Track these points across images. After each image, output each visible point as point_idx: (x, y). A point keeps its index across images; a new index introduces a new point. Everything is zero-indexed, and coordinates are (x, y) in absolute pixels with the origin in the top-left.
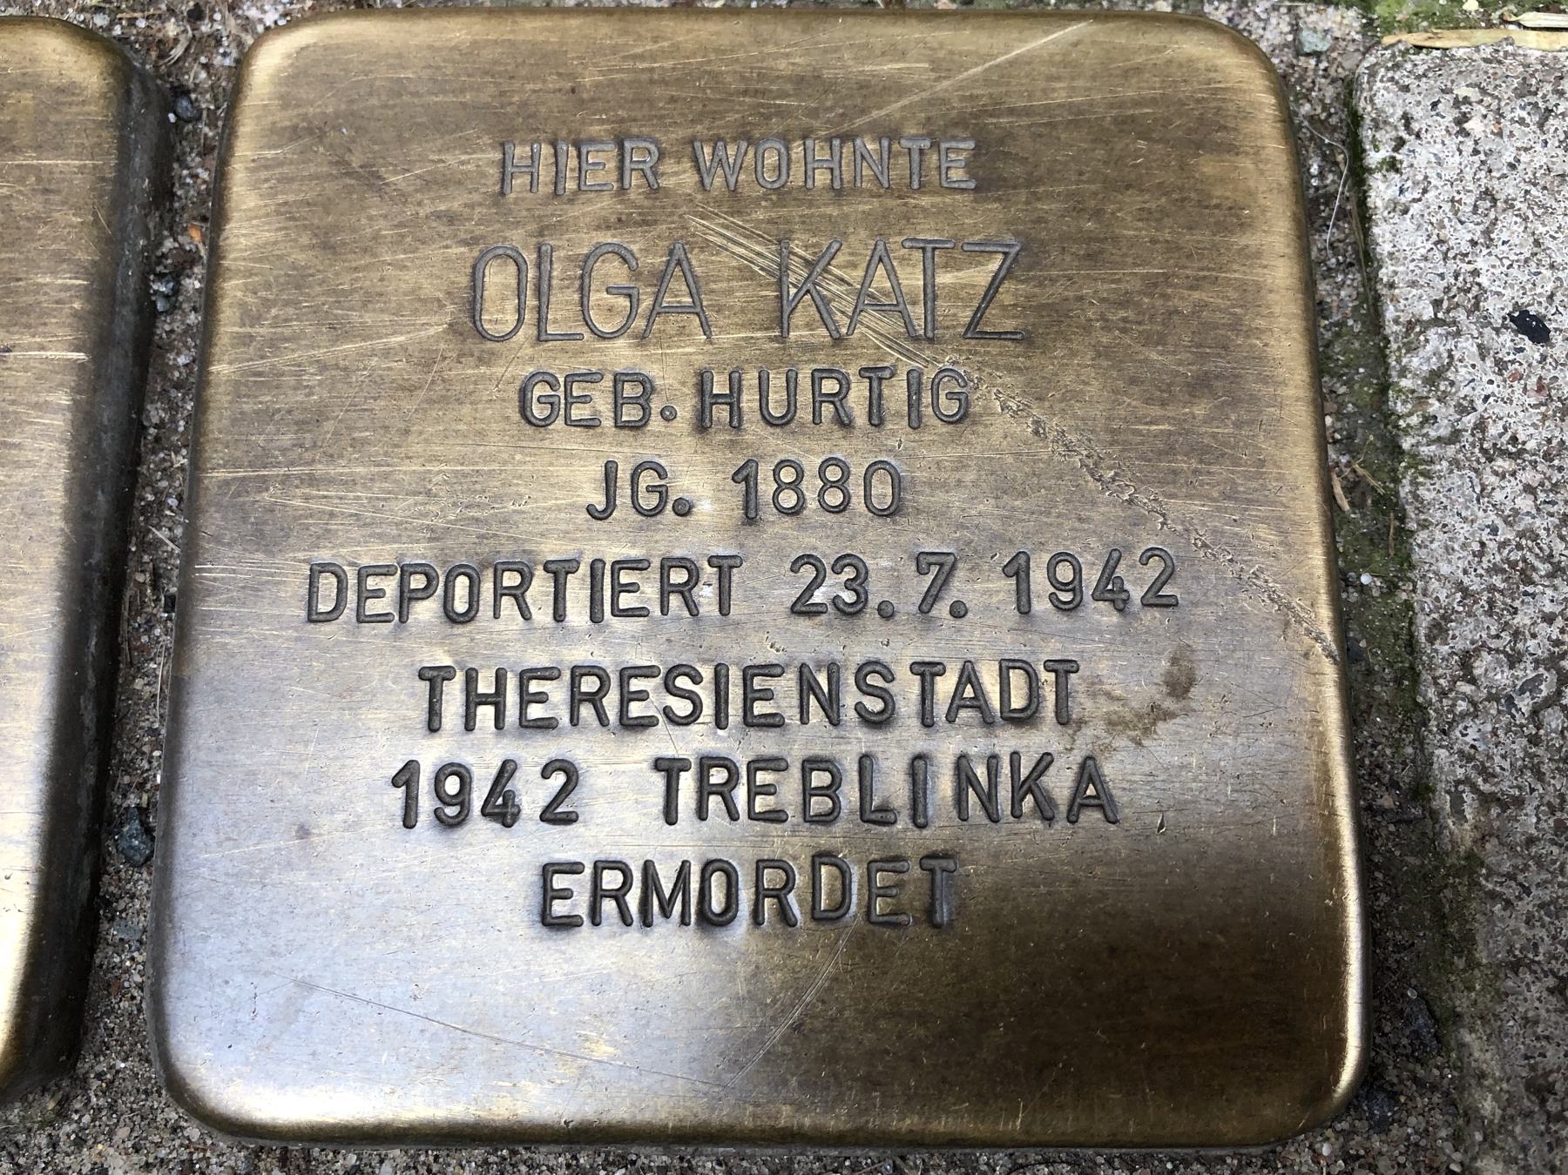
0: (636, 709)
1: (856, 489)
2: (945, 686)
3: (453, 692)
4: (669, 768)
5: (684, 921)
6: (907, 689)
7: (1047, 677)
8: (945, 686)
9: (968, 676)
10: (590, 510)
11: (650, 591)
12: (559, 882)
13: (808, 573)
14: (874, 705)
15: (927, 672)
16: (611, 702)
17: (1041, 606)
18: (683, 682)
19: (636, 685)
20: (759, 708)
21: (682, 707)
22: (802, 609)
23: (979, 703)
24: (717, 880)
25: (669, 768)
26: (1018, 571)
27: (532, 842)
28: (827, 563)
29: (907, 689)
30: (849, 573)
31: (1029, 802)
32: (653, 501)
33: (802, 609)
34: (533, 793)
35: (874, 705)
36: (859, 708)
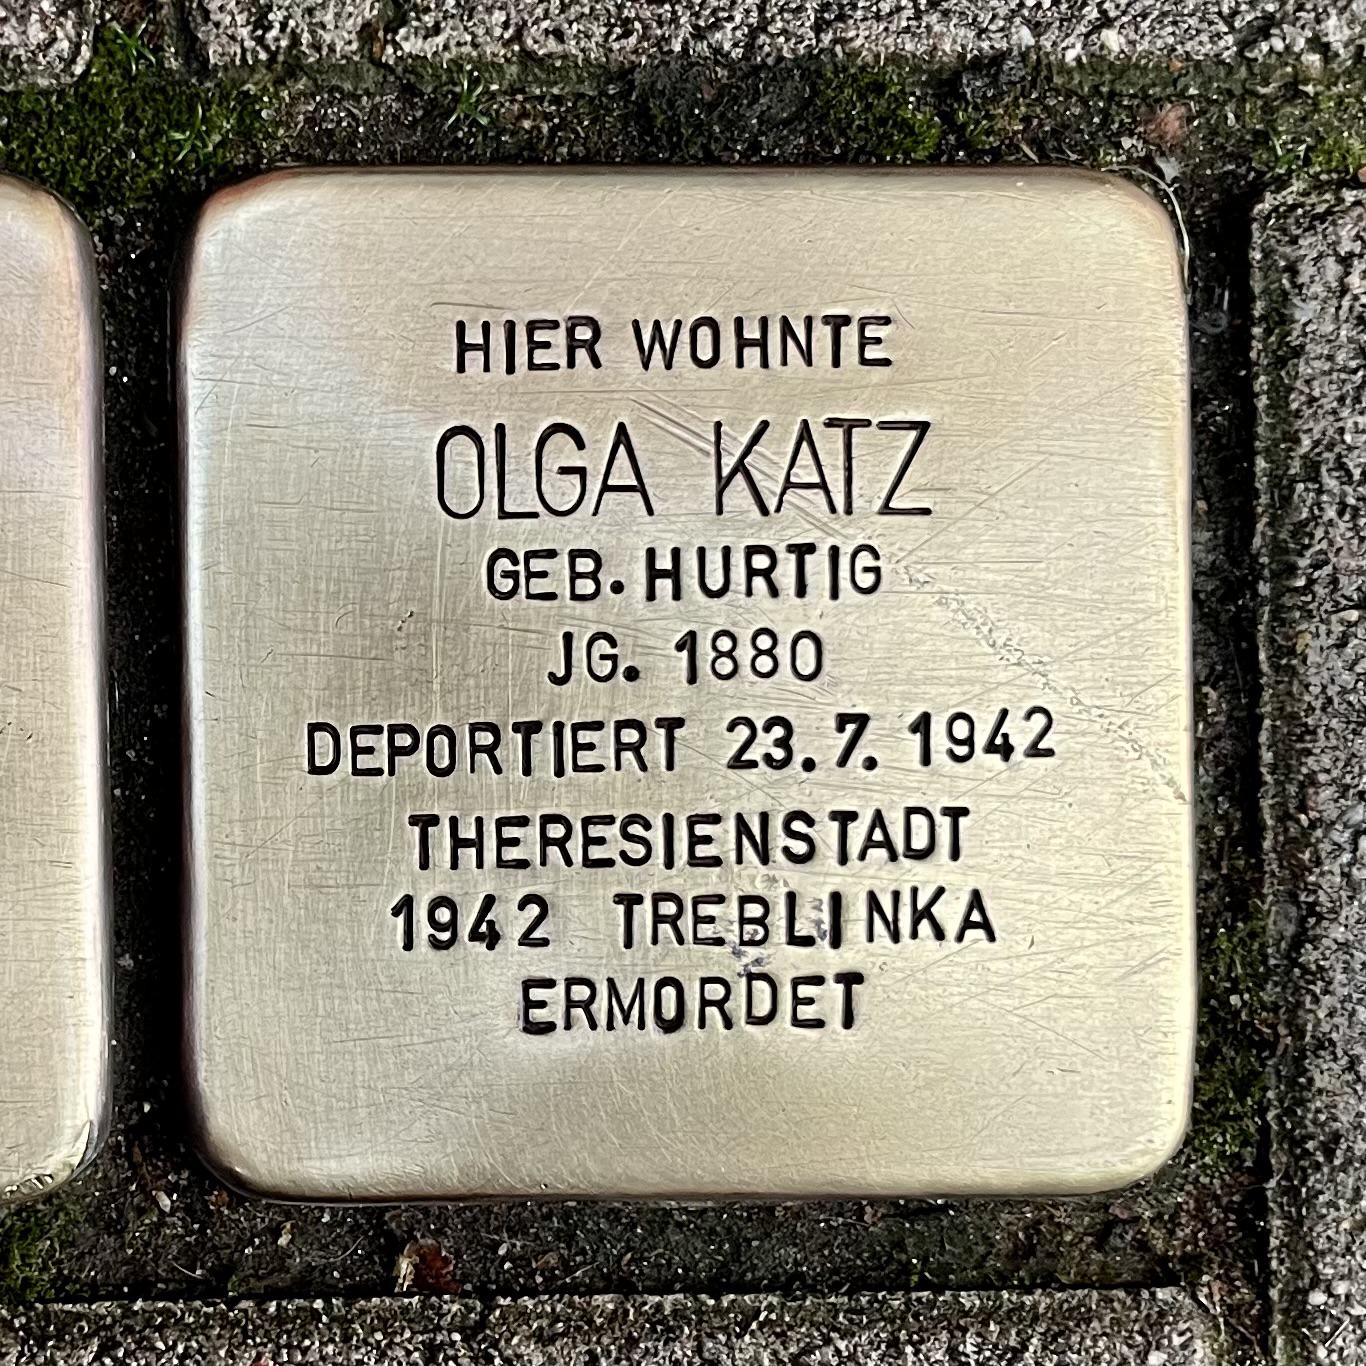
0: (596, 852)
1: (783, 652)
2: (857, 833)
3: (441, 835)
4: (630, 901)
5: (642, 1025)
6: (827, 834)
7: (944, 824)
8: (857, 833)
9: (878, 820)
10: (552, 676)
11: (605, 754)
12: (536, 994)
13: (743, 732)
14: (800, 847)
15: (845, 818)
16: (575, 847)
17: (939, 756)
18: (636, 829)
19: (595, 831)
20: (702, 851)
21: (637, 851)
22: (738, 762)
23: (887, 843)
24: (669, 993)
25: (630, 901)
26: (922, 725)
27: (514, 962)
28: (759, 725)
29: (827, 834)
30: (778, 732)
31: (925, 927)
32: (605, 668)
33: (738, 762)
34: (513, 922)
35: (800, 847)
36: (786, 850)
